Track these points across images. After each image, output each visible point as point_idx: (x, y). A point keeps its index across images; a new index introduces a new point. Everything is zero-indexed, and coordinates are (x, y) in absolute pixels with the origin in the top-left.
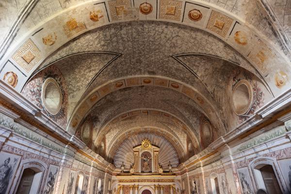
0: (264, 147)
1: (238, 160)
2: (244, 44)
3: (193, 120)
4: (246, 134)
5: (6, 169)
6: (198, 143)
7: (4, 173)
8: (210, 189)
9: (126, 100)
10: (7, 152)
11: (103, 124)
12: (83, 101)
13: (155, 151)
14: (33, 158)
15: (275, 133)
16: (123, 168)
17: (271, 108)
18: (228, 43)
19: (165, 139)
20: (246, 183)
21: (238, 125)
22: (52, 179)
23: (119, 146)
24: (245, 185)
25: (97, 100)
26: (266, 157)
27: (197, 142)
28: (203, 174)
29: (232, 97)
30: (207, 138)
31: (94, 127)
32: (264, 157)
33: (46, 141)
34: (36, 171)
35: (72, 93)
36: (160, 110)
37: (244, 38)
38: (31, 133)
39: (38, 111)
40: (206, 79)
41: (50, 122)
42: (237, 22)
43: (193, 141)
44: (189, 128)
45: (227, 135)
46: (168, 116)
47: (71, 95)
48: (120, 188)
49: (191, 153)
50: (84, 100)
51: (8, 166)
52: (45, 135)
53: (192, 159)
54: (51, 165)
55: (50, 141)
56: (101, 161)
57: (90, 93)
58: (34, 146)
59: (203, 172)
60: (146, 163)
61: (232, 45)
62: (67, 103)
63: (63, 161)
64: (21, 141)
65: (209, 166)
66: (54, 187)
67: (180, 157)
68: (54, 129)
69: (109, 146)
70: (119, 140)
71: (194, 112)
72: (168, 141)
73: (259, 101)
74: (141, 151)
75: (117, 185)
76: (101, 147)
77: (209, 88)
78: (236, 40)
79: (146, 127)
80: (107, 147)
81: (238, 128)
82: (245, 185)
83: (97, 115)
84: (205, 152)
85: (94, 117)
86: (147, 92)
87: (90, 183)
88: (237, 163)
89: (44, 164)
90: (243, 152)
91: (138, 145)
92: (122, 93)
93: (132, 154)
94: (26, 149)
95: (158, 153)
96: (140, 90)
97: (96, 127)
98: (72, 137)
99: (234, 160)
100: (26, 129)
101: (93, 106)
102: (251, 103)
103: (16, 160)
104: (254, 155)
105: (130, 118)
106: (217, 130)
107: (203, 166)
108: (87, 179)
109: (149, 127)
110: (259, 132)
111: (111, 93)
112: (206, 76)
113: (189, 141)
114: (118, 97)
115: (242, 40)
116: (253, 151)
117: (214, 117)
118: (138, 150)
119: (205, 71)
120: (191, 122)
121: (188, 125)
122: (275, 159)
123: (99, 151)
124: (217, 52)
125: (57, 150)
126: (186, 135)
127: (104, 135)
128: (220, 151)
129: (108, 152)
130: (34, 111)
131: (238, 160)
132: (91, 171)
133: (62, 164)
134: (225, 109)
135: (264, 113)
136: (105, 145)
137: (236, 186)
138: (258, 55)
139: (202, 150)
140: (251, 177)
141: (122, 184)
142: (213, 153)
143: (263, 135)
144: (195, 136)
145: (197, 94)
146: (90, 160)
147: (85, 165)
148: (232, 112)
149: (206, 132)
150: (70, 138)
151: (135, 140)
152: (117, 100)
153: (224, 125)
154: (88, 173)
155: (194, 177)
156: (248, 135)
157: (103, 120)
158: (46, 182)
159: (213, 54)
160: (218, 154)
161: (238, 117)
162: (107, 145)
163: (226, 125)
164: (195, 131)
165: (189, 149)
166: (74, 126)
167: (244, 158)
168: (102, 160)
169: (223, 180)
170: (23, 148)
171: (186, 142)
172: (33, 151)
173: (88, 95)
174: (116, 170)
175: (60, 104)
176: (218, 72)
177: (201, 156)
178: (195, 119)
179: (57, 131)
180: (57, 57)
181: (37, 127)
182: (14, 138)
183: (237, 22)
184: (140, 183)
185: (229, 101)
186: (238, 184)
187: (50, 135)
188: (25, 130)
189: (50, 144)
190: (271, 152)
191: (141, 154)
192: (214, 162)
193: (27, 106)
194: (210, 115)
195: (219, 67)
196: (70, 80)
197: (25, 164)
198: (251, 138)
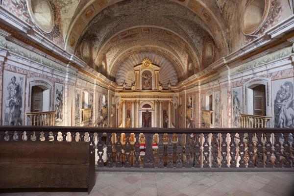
0: (264, 68)
3: (196, 40)
4: (249, 55)
5: (15, 87)
6: (199, 63)
8: (203, 105)
9: (125, 15)
10: (10, 71)
11: (103, 43)
12: (77, 17)
13: (156, 70)
14: (37, 77)
15: (279, 54)
16: (124, 85)
17: (285, 27)
19: (166, 59)
20: (237, 100)
21: (242, 45)
22: (59, 95)
23: (118, 66)
24: (236, 102)
25: (94, 16)
26: (262, 78)
27: (198, 62)
28: (200, 92)
29: (243, 13)
30: (208, 58)
31: (93, 46)
32: (260, 78)
33: (46, 60)
34: (43, 88)
35: (63, 7)
36: (162, 28)
38: (28, 53)
39: (29, 29)
41: (44, 40)
43: (194, 61)
44: (192, 48)
45: (229, 56)
46: (170, 34)
47: (63, 9)
48: (123, 102)
49: (191, 73)
50: (79, 15)
51: (16, 84)
53: (191, 78)
54: (56, 83)
55: (50, 61)
56: (103, 80)
57: (85, 7)
58: (36, 66)
59: (200, 90)
60: (146, 81)
62: (60, 19)
63: (67, 80)
64: (20, 61)
65: (207, 85)
66: (63, 102)
67: (179, 76)
68: (51, 48)
69: (110, 66)
70: (120, 59)
71: (199, 31)
72: (169, 61)
73: (273, 19)
74: (142, 70)
75: (120, 100)
76: (102, 66)
79: (147, 46)
80: (108, 68)
81: (241, 49)
82: (236, 102)
83: (95, 33)
84: (204, 72)
85: (92, 36)
86: (148, 6)
87: (95, 98)
88: (233, 83)
89: (49, 82)
90: (242, 72)
91: (139, 64)
92: (121, 7)
93: (132, 72)
94: (28, 68)
95: (158, 72)
96: (141, 4)
97: (95, 46)
98: (72, 57)
99: (231, 80)
100: (22, 48)
101: (89, 23)
102: (264, 21)
103: (21, 79)
104: (252, 76)
105: (130, 36)
106: (220, 50)
107: (201, 85)
108: (92, 95)
109: (150, 46)
110: (263, 53)
111: (109, 7)
113: (190, 60)
114: (117, 12)
116: (251, 72)
117: (220, 37)
118: (138, 69)
120: (194, 41)
121: (190, 44)
122: (269, 80)
123: (100, 70)
125: (59, 70)
126: (187, 56)
127: (104, 55)
128: (219, 71)
129: (109, 72)
130: (24, 28)
131: (235, 80)
132: (95, 89)
133: (66, 82)
134: (233, 28)
135: (274, 33)
136: (106, 65)
137: (228, 102)
139: (202, 70)
140: (243, 95)
141: (124, 99)
142: (212, 73)
143: (266, 56)
144: (196, 56)
145: (204, 9)
146: (92, 78)
147: (89, 83)
148: (239, 31)
149: (209, 53)
150: (70, 57)
151: (136, 59)
152: (115, 15)
153: (228, 45)
154: (93, 90)
155: (191, 94)
156: (251, 56)
157: (102, 38)
158: (55, 98)
160: (216, 74)
161: (245, 37)
162: (108, 64)
163: (230, 46)
164: (197, 51)
165: (189, 68)
166: (72, 45)
167: (241, 78)
168: (104, 78)
169: (217, 97)
170: (24, 67)
171: (186, 62)
172: (35, 71)
173: (83, 10)
174: (118, 87)
175: (52, 19)
177: (200, 75)
178: (199, 38)
179: (55, 50)
181: (33, 46)
182: (12, 58)
184: (140, 99)
185: (239, 20)
186: (230, 101)
187: (49, 54)
188: (21, 49)
191: (141, 72)
192: (211, 81)
193: (15, 21)
194: (214, 35)
197: (32, 82)
198: (252, 60)
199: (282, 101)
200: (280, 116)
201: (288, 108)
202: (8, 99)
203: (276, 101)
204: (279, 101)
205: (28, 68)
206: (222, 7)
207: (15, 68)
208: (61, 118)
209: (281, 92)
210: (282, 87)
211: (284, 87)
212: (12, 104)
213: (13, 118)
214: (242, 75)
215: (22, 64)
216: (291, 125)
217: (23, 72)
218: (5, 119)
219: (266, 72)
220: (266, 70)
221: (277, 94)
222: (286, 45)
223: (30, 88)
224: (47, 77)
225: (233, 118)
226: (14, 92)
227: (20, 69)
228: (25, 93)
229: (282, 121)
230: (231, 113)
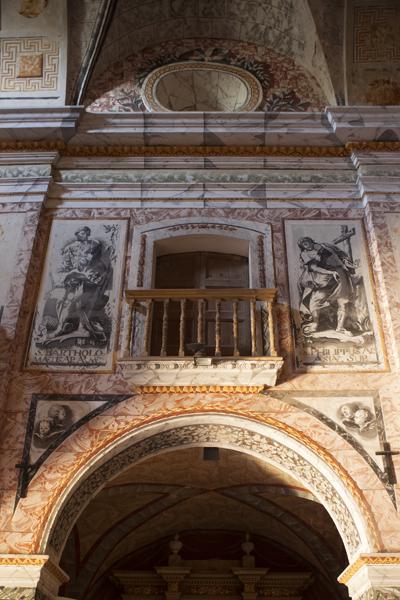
7: (87, 252)
14: (178, 216)
35: (290, 43)
39: (78, 115)
41: (150, 120)
47: (295, 48)
52: (200, 161)
63: (365, 201)
98: (330, 117)
103: (108, 229)
130: (65, 120)
150: (329, 126)
170: (120, 204)
180: (94, 10)
189: (245, 177)
193: (37, 120)
196: (250, 26)
202: (63, 272)
205: (138, 204)
207: (89, 211)
208: (355, 331)
212: (71, 283)
213: (73, 309)
215: (111, 199)
217: (119, 214)
218: (46, 310)
223: (144, 244)
224: (230, 212)
226: (83, 255)
227: (105, 211)
228: (127, 258)
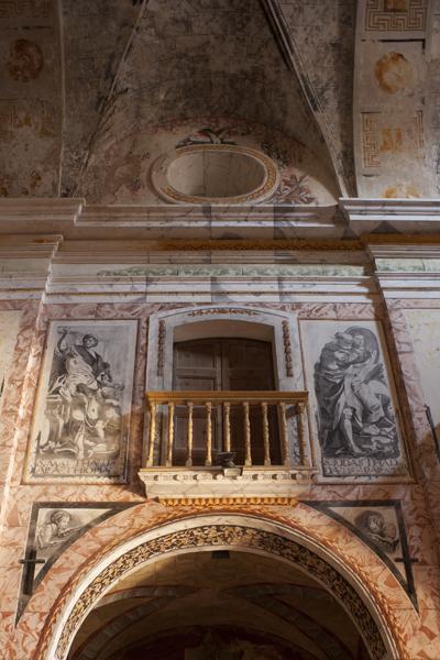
1: (75, 299)
2: (387, 88)
17: (392, 213)
18: (359, 49)
29: (164, 157)
37: (399, 79)
40: (147, 38)
42: (423, 40)
45: (119, 210)
61: (360, 60)
77: (124, 67)
78: (379, 63)
104: (207, 298)
110: (270, 255)
112: (160, 35)
115: (388, 78)
116: (207, 287)
119: (175, 21)
124: (301, 29)
131: (75, 299)
138: (387, 132)
159: (287, 21)
176: (193, 71)
183: (423, 40)
186: (32, 361)
190: (288, 300)
195: (217, 64)
198: (209, 262)
199: (345, 365)
200: (342, 401)
201: (366, 382)
203: (319, 367)
204: (333, 366)
206: (119, 89)
209: (340, 347)
210: (338, 336)
211: (349, 337)
214: (142, 287)
216: (381, 418)
219: (276, 299)
220: (281, 293)
221: (323, 350)
222: (346, 261)
225: (42, 425)
229: (349, 412)
230: (33, 407)
